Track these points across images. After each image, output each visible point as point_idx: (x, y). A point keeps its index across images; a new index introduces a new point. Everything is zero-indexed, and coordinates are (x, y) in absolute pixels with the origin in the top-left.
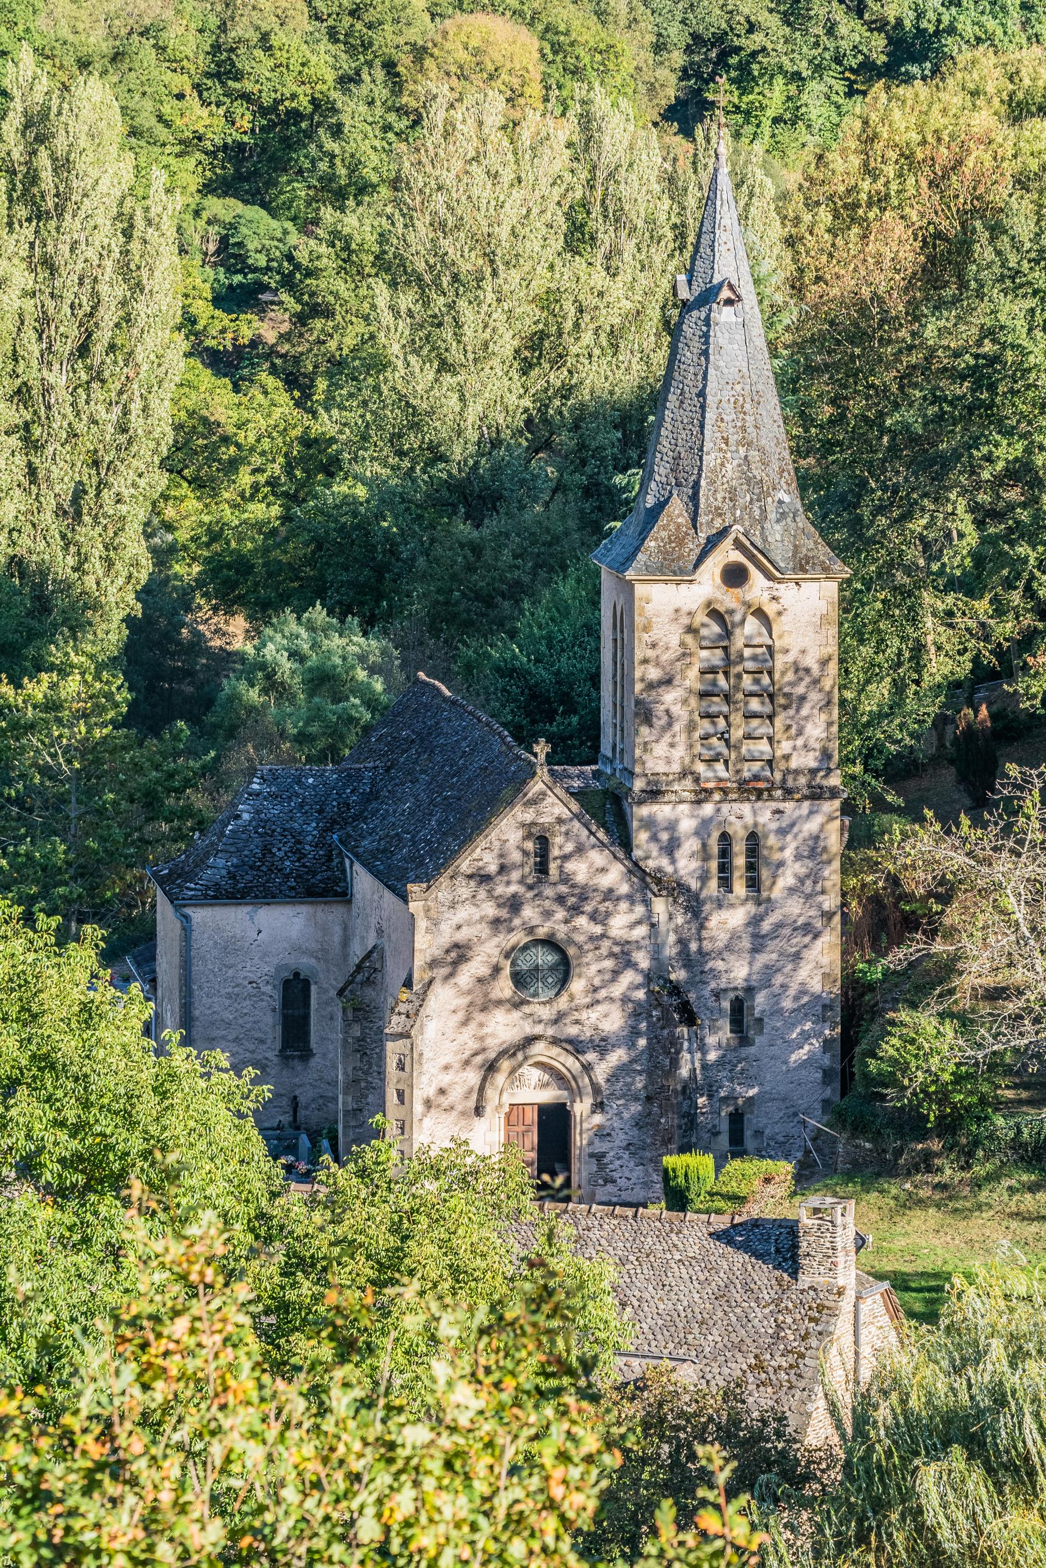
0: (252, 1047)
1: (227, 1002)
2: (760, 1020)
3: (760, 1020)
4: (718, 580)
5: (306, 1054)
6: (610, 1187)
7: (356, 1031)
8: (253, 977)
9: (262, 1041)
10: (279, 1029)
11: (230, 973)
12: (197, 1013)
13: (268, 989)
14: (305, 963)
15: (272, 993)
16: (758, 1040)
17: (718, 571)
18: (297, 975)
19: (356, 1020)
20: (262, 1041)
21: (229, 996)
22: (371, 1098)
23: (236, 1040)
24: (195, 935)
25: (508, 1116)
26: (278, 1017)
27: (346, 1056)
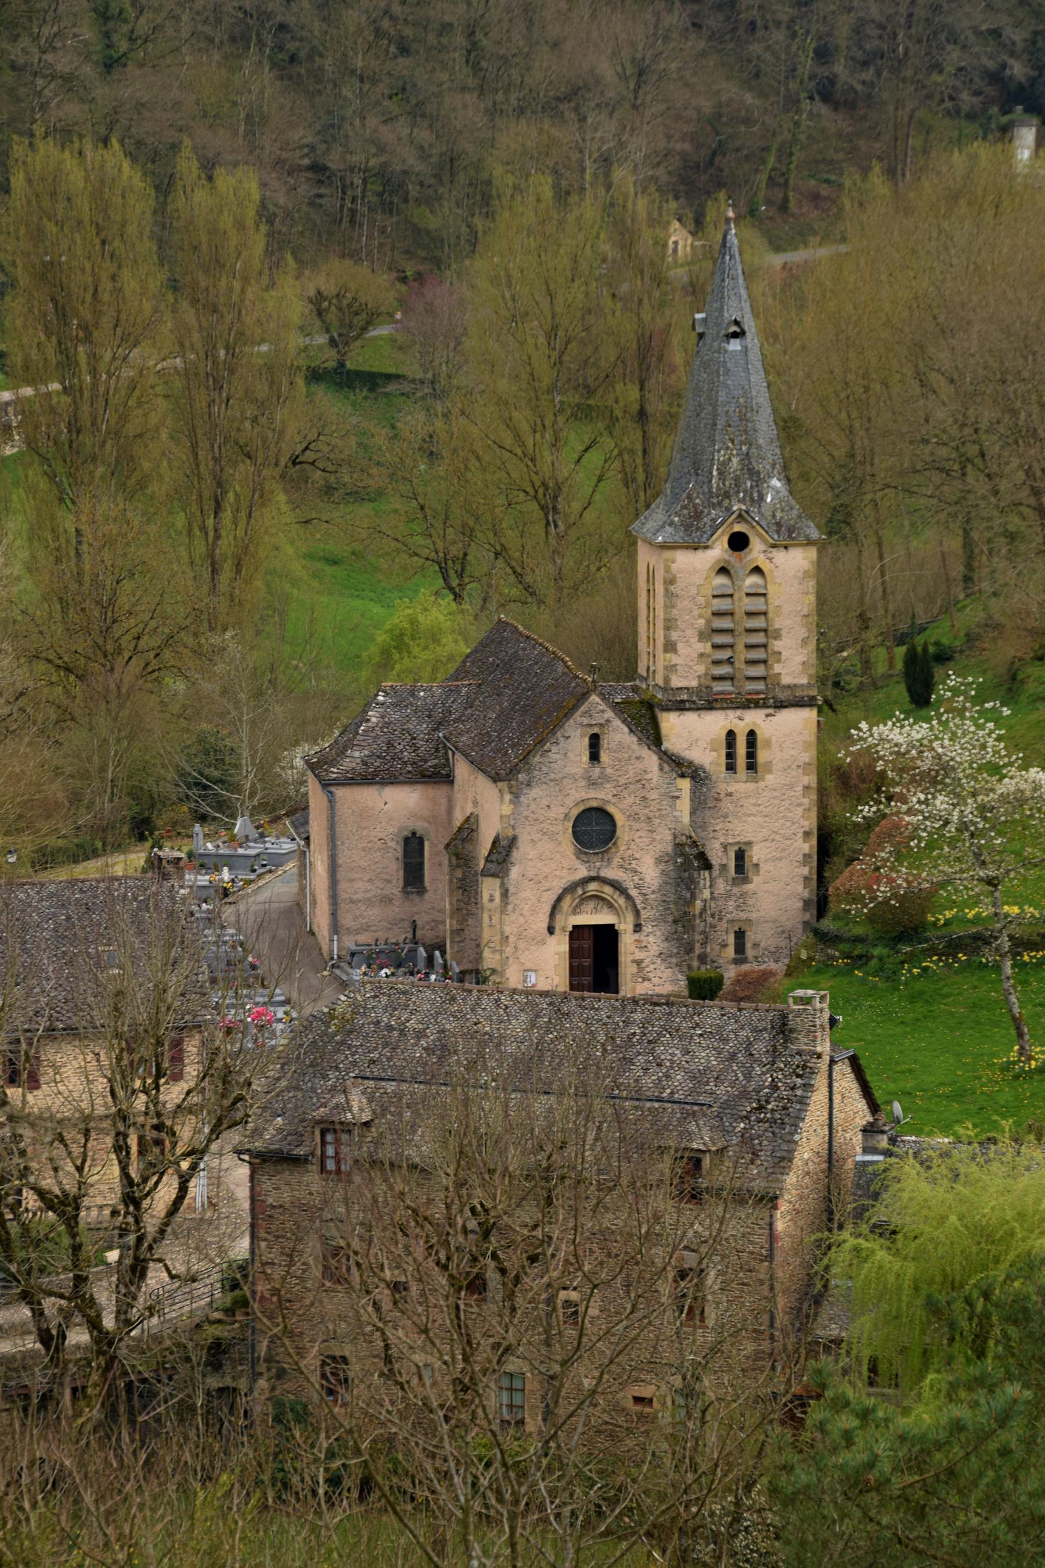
0: (381, 886)
1: (363, 854)
2: (757, 865)
3: (757, 865)
4: (726, 545)
5: (422, 891)
6: (646, 983)
7: (459, 874)
8: (381, 836)
9: (389, 881)
10: (401, 873)
11: (365, 833)
12: (340, 862)
13: (393, 844)
14: (420, 826)
15: (397, 849)
16: (756, 879)
17: (726, 539)
18: (414, 834)
19: (458, 866)
20: (389, 881)
21: (364, 849)
22: (470, 922)
23: (370, 880)
24: (338, 805)
25: (571, 933)
26: (401, 865)
27: (451, 891)
